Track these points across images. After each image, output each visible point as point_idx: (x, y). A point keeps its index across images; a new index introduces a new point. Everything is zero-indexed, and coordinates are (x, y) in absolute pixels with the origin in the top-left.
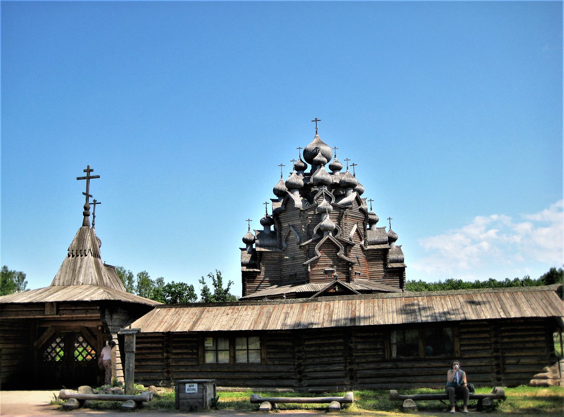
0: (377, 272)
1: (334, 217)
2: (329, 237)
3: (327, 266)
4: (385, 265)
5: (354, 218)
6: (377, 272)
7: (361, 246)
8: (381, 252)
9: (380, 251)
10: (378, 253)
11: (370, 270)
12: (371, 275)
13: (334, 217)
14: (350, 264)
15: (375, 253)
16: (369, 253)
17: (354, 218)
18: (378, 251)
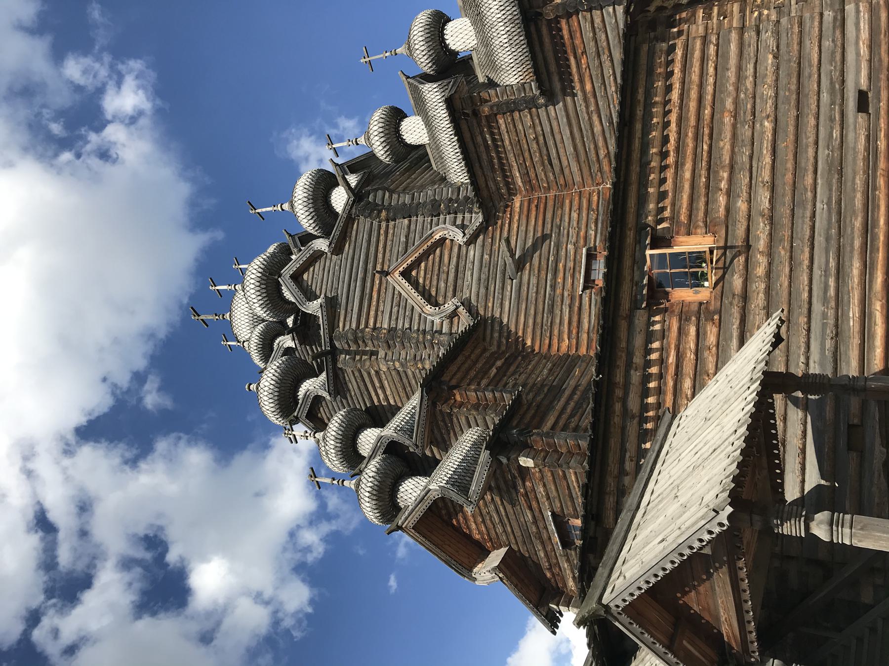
0: (580, 145)
1: (377, 384)
2: (412, 526)
3: (545, 536)
4: (531, 104)
5: (368, 284)
6: (580, 145)
7: (471, 241)
8: (482, 133)
9: (479, 139)
10: (487, 147)
11: (578, 179)
12: (600, 170)
13: (377, 384)
14: (504, 460)
15: (491, 159)
16: (498, 189)
17: (368, 284)
18: (482, 149)
